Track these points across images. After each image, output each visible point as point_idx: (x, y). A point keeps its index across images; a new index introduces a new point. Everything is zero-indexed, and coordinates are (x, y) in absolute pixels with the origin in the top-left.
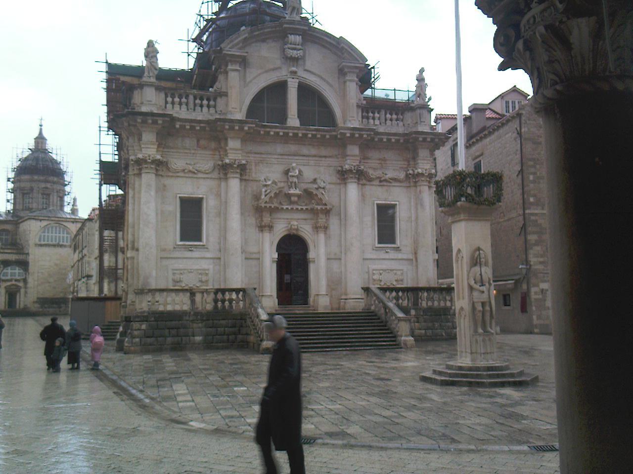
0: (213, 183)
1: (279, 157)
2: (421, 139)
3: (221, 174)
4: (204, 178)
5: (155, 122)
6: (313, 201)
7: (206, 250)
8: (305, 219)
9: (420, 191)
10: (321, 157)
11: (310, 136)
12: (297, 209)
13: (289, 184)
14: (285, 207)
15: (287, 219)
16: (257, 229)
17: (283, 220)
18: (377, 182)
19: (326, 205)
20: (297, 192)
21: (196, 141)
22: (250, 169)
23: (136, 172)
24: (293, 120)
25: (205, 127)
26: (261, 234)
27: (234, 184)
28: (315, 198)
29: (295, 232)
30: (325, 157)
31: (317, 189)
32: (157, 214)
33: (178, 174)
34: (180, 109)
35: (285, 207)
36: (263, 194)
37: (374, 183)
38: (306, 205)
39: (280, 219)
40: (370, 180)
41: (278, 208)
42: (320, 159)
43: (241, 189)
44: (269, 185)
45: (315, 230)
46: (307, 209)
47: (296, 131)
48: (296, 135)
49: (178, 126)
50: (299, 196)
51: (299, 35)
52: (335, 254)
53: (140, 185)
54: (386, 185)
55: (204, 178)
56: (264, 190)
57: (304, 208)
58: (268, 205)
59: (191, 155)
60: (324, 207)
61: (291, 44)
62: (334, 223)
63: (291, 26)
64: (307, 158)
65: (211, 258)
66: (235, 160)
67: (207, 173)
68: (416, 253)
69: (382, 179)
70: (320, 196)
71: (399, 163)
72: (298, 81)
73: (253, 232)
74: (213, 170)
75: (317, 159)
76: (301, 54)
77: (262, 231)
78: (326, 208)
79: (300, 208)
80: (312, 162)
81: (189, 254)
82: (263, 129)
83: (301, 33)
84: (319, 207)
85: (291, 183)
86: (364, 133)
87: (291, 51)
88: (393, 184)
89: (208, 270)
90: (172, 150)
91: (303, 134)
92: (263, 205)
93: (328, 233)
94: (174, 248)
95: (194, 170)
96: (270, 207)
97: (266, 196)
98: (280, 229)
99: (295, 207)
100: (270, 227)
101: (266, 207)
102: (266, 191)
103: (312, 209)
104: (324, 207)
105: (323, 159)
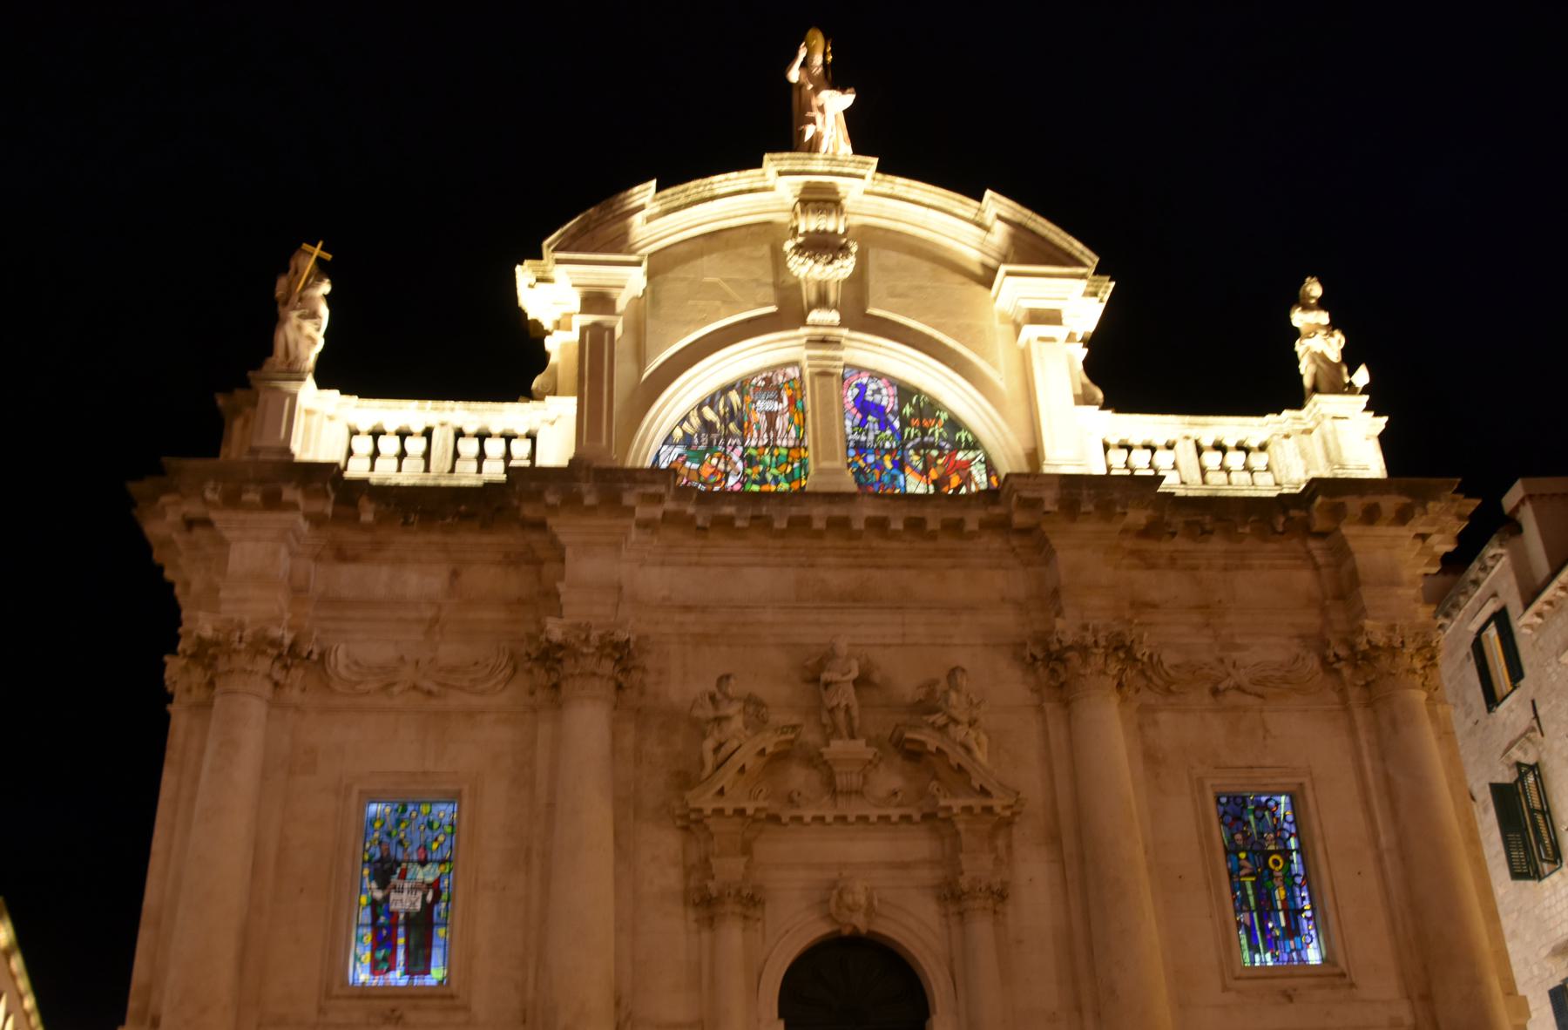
3: (541, 695)
4: (470, 714)
7: (460, 1017)
8: (904, 866)
9: (1394, 722)
13: (826, 719)
14: (808, 815)
16: (692, 915)
19: (984, 792)
22: (660, 672)
23: (199, 694)
26: (706, 935)
27: (589, 721)
29: (860, 922)
31: (942, 729)
32: (256, 869)
34: (399, 470)
35: (808, 815)
38: (899, 805)
41: (775, 819)
43: (615, 750)
45: (952, 909)
47: (838, 511)
48: (840, 525)
53: (201, 752)
55: (470, 714)
56: (709, 744)
57: (894, 813)
62: (1034, 875)
66: (588, 626)
67: (482, 693)
68: (1427, 997)
70: (956, 756)
73: (672, 930)
77: (711, 919)
78: (988, 810)
84: (957, 804)
85: (831, 711)
94: (321, 1010)
95: (427, 684)
96: (740, 812)
99: (853, 809)
100: (752, 902)
101: (719, 812)
102: (720, 745)
104: (976, 802)
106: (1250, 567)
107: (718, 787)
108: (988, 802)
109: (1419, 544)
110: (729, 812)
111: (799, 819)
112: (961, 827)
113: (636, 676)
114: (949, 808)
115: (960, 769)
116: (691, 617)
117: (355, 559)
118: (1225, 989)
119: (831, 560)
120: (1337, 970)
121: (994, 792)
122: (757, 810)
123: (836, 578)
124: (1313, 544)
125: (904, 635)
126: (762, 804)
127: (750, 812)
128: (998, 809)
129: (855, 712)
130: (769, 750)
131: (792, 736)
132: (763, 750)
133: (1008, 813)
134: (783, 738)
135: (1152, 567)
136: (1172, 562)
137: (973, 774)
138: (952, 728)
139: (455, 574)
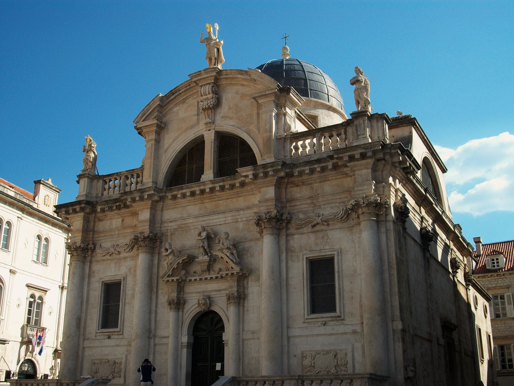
0: (130, 263)
2: (346, 159)
5: (75, 211)
7: (121, 337)
11: (218, 188)
12: (206, 279)
14: (193, 279)
15: (199, 293)
17: (194, 295)
18: (308, 229)
21: (120, 220)
24: (208, 175)
25: (120, 205)
33: (105, 258)
37: (305, 230)
39: (192, 293)
40: (300, 227)
46: (217, 278)
47: (202, 188)
49: (99, 210)
51: (209, 84)
52: (253, 333)
54: (322, 231)
55: (125, 258)
59: (116, 236)
60: (229, 273)
61: (202, 96)
63: (199, 78)
64: (224, 216)
65: (124, 346)
68: (362, 323)
69: (315, 222)
71: (339, 197)
72: (214, 131)
74: (132, 248)
76: (212, 103)
79: (214, 276)
80: (230, 218)
81: (108, 342)
82: (171, 194)
83: (213, 81)
86: (269, 169)
87: (202, 103)
88: (330, 227)
89: (122, 359)
90: (101, 235)
91: (211, 188)
93: (246, 305)
94: (96, 336)
96: (173, 280)
98: (193, 307)
105: (242, 212)
106: (329, 180)
109: (383, 162)
111: (190, 280)
117: (102, 220)
118: (304, 323)
119: (207, 201)
120: (337, 315)
123: (209, 205)
124: (345, 169)
135: (297, 186)
136: (303, 184)
139: (123, 220)
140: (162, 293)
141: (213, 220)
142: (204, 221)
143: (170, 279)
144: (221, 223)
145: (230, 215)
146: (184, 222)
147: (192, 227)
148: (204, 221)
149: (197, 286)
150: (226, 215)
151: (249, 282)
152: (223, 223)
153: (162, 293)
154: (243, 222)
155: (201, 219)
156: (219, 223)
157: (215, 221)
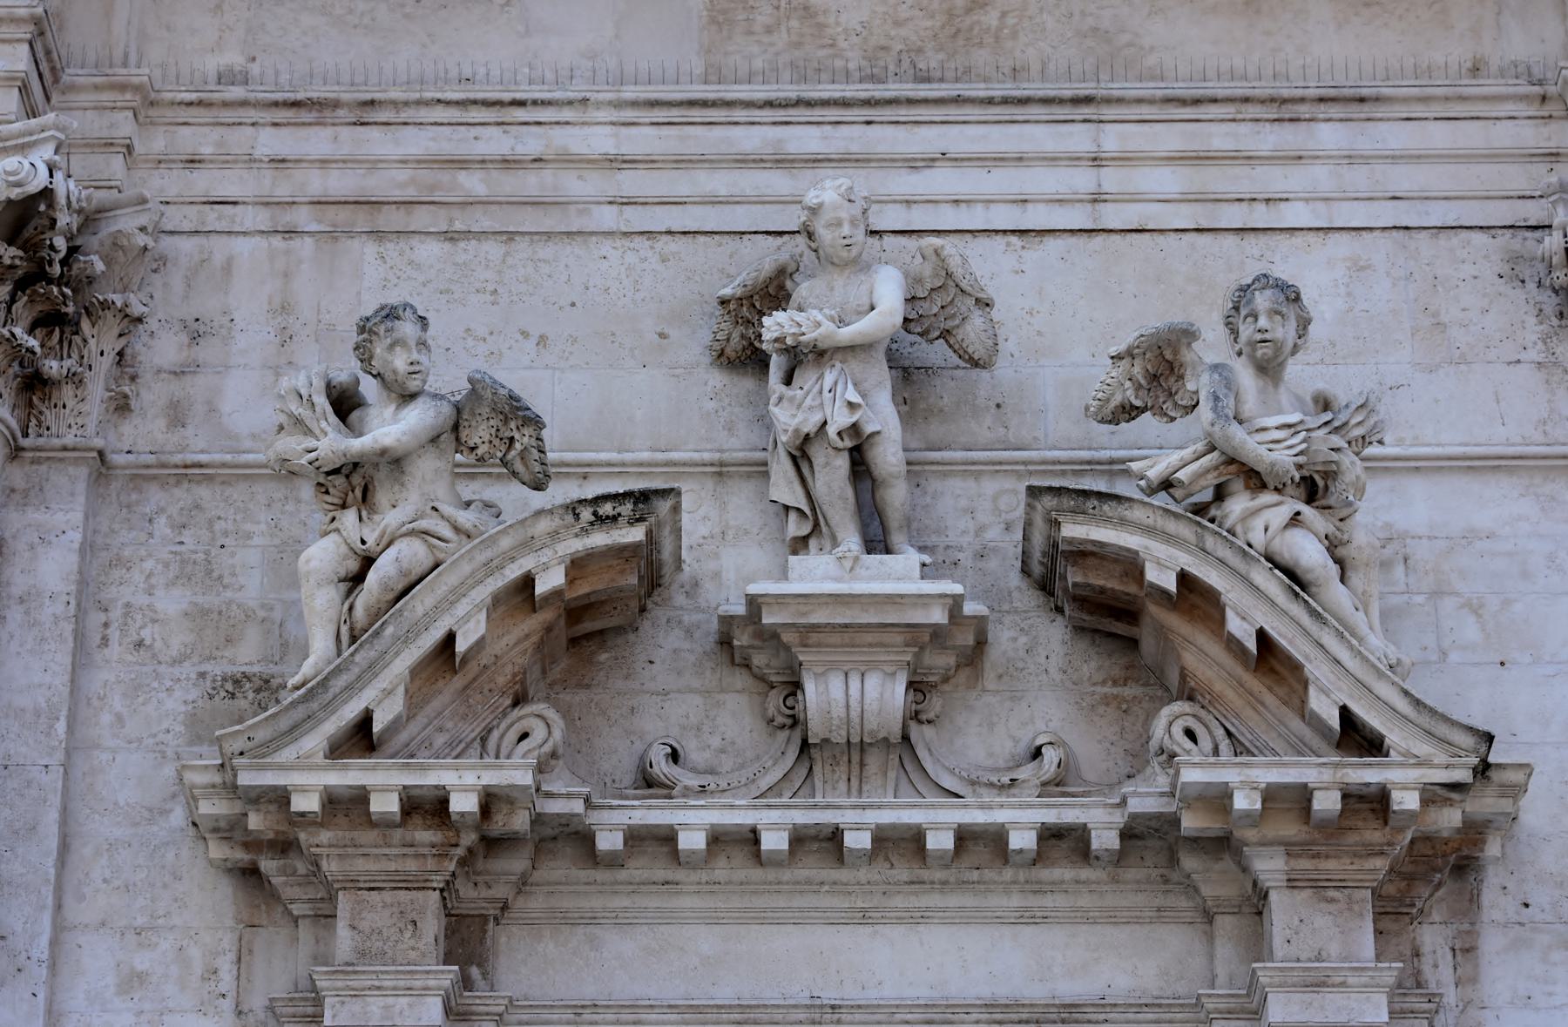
1: (645, 140)
6: (1169, 721)
10: (1284, 107)
13: (785, 488)
14: (693, 825)
19: (1356, 738)
20: (898, 574)
28: (1200, 655)
30: (1356, 102)
35: (693, 825)
36: (321, 607)
42: (1270, 138)
44: (394, 462)
50: (944, 659)
56: (323, 555)
57: (1022, 821)
58: (384, 782)
60: (1328, 778)
64: (1078, 138)
75: (1220, 137)
80: (1167, 180)
85: (801, 455)
92: (309, 778)
97: (353, 635)
103: (1147, 838)
104: (1328, 778)
105: (1329, 135)
107: (350, 712)
108: (1366, 774)
110: (386, 804)
112: (1269, 866)
113: (100, 340)
114: (1219, 799)
115: (1267, 654)
116: (316, 141)
121: (1394, 736)
122: (490, 801)
125: (1097, 199)
126: (516, 774)
127: (463, 804)
128: (1405, 801)
129: (888, 456)
130: (550, 580)
131: (636, 534)
132: (528, 582)
133: (1449, 819)
134: (600, 539)
137: (1316, 669)
138: (1238, 505)
140: (132, 981)
141: (914, 164)
142: (783, 162)
143: (384, 782)
144: (1036, 217)
145: (1170, 138)
146: (494, 142)
147: (607, 218)
148: (783, 162)
149: (705, 940)
150: (1112, 139)
151: (1492, 943)
152: (1076, 217)
153: (132, 981)
154: (1342, 245)
155: (751, 139)
156: (1004, 217)
157: (942, 181)
